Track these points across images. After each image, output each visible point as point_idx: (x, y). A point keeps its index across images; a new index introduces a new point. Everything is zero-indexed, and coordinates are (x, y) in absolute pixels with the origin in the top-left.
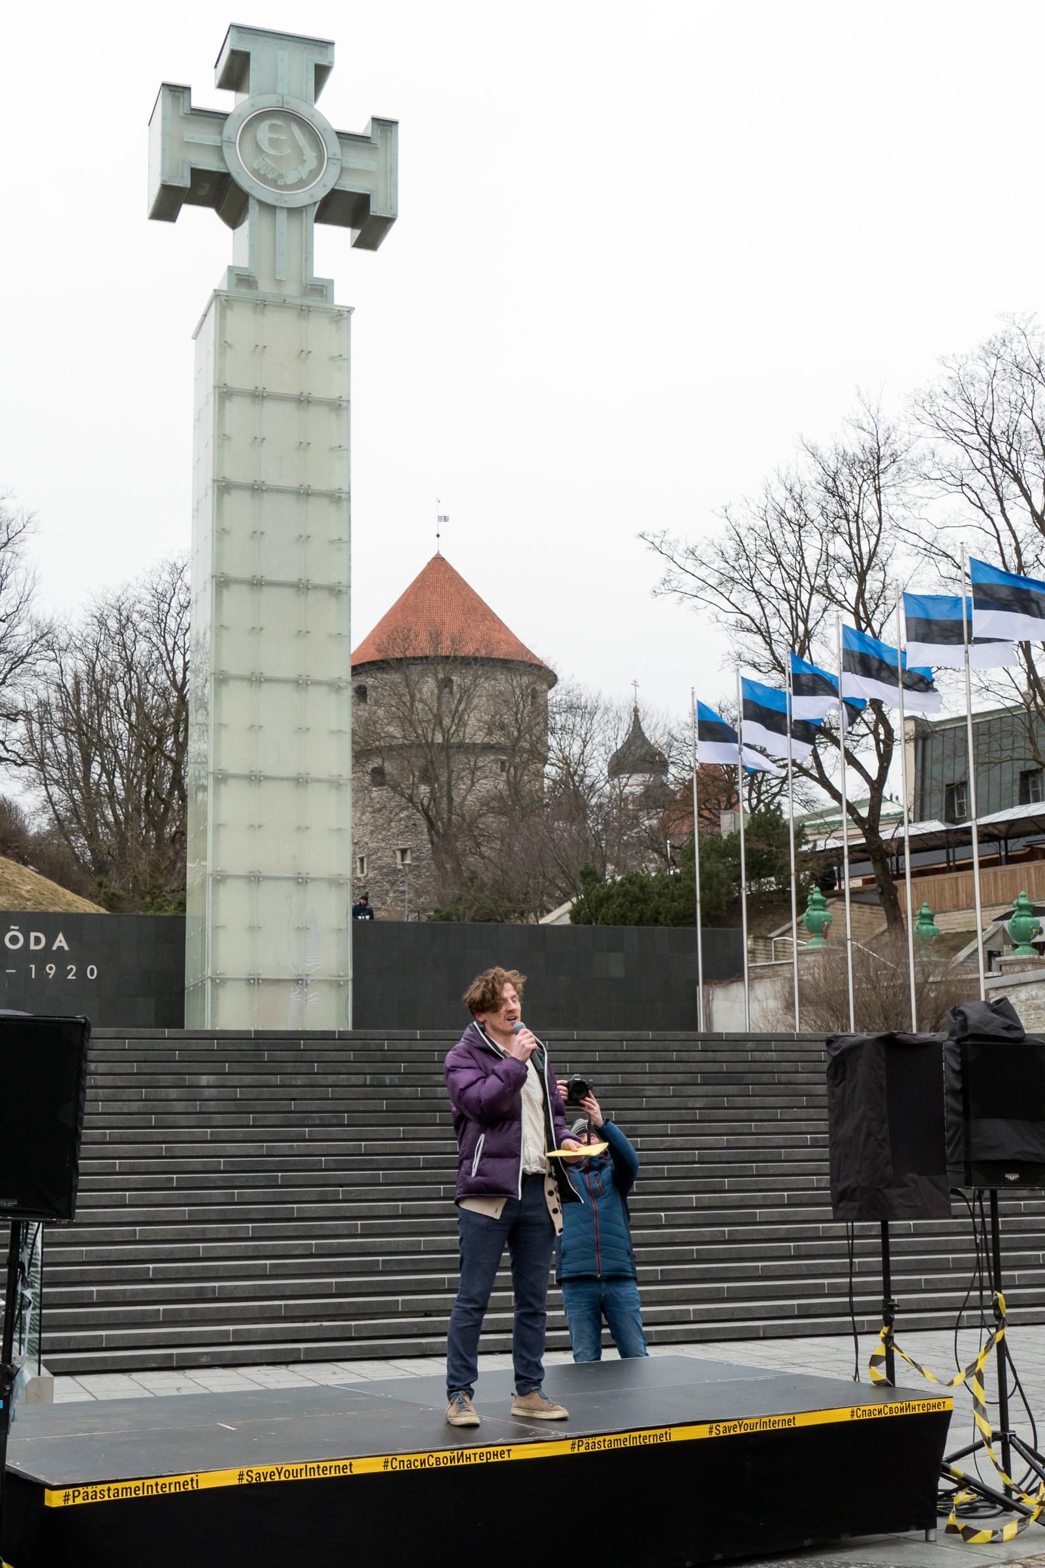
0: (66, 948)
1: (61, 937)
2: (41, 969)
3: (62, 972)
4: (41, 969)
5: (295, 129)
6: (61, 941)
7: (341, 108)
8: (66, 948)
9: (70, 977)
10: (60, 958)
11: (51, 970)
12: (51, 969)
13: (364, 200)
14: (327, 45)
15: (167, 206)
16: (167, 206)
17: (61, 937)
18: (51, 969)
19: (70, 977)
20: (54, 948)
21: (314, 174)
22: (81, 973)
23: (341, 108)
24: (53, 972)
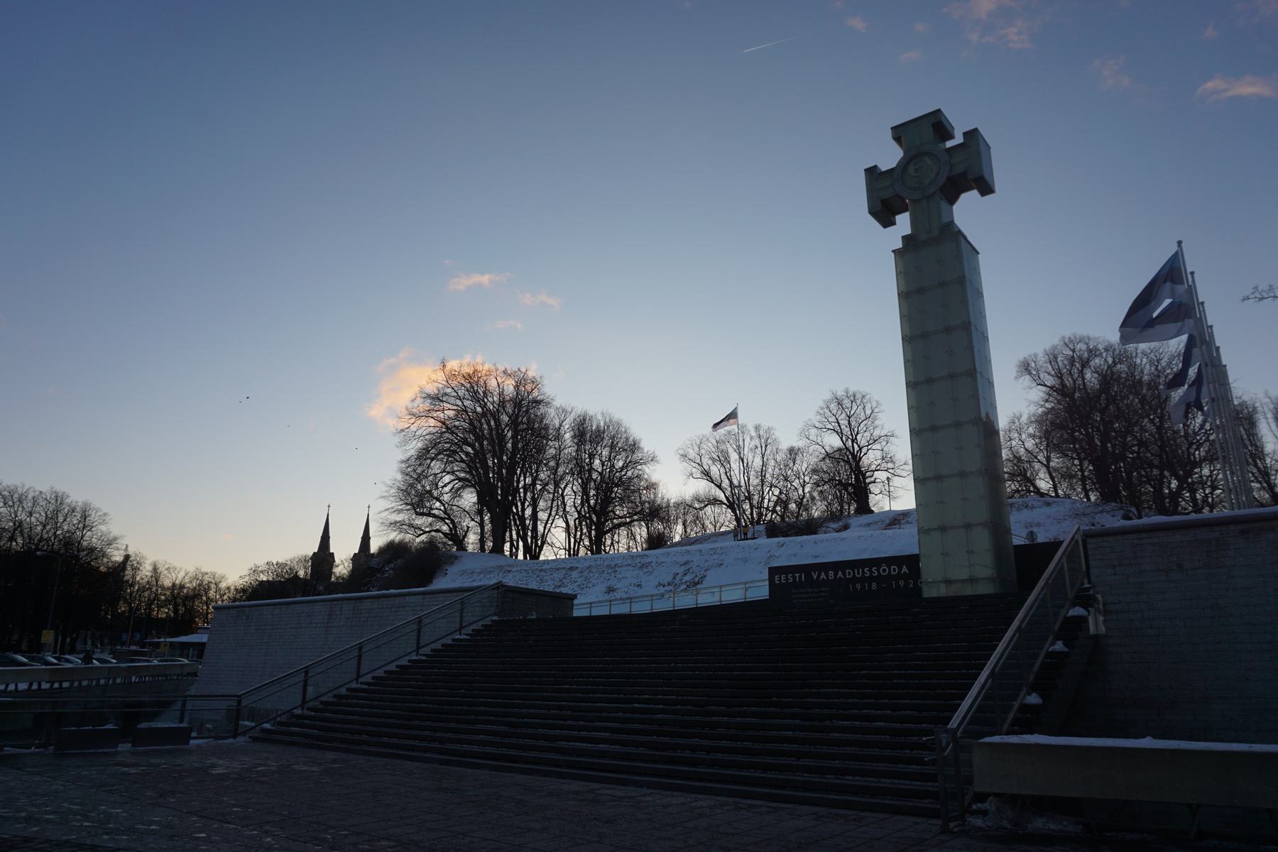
2: (897, 583)
4: (897, 583)
5: (927, 159)
6: (905, 569)
11: (902, 583)
13: (964, 174)
21: (938, 174)
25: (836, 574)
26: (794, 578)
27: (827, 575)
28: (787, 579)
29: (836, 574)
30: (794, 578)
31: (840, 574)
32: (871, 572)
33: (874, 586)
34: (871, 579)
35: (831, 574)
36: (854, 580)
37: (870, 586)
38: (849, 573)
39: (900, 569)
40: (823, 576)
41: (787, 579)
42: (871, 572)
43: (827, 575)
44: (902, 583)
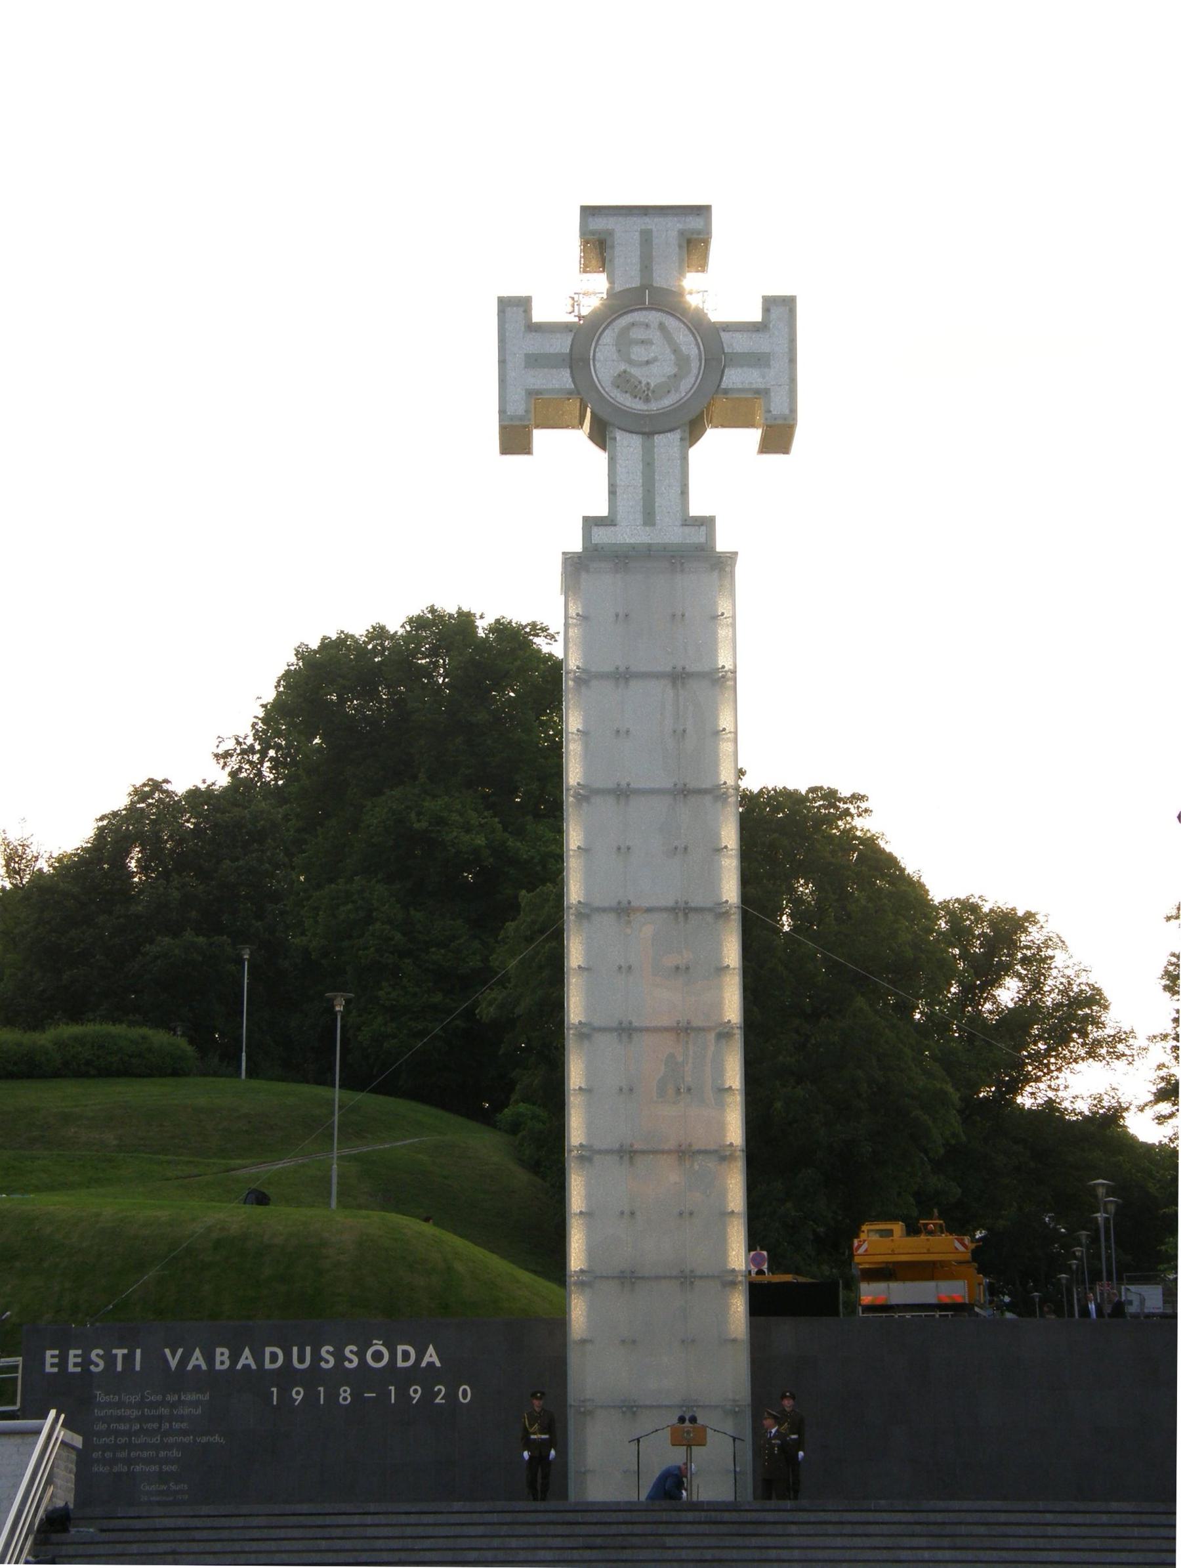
0: (438, 1364)
1: (431, 1350)
2: (403, 1394)
3: (429, 1395)
4: (403, 1394)
6: (431, 1356)
7: (721, 291)
8: (438, 1364)
9: (437, 1401)
10: (427, 1376)
11: (416, 1393)
12: (416, 1391)
14: (703, 211)
15: (515, 440)
16: (515, 440)
17: (431, 1350)
18: (416, 1391)
19: (437, 1401)
20: (424, 1364)
22: (451, 1396)
23: (721, 291)
24: (418, 1396)
25: (235, 1357)
26: (110, 1360)
27: (210, 1358)
28: (86, 1362)
29: (235, 1357)
30: (110, 1360)
31: (247, 1358)
32: (340, 1357)
33: (345, 1394)
34: (341, 1374)
35: (222, 1356)
36: (287, 1376)
37: (332, 1396)
38: (274, 1357)
39: (420, 1355)
40: (197, 1359)
41: (86, 1362)
42: (340, 1357)
43: (210, 1358)
44: (416, 1393)
